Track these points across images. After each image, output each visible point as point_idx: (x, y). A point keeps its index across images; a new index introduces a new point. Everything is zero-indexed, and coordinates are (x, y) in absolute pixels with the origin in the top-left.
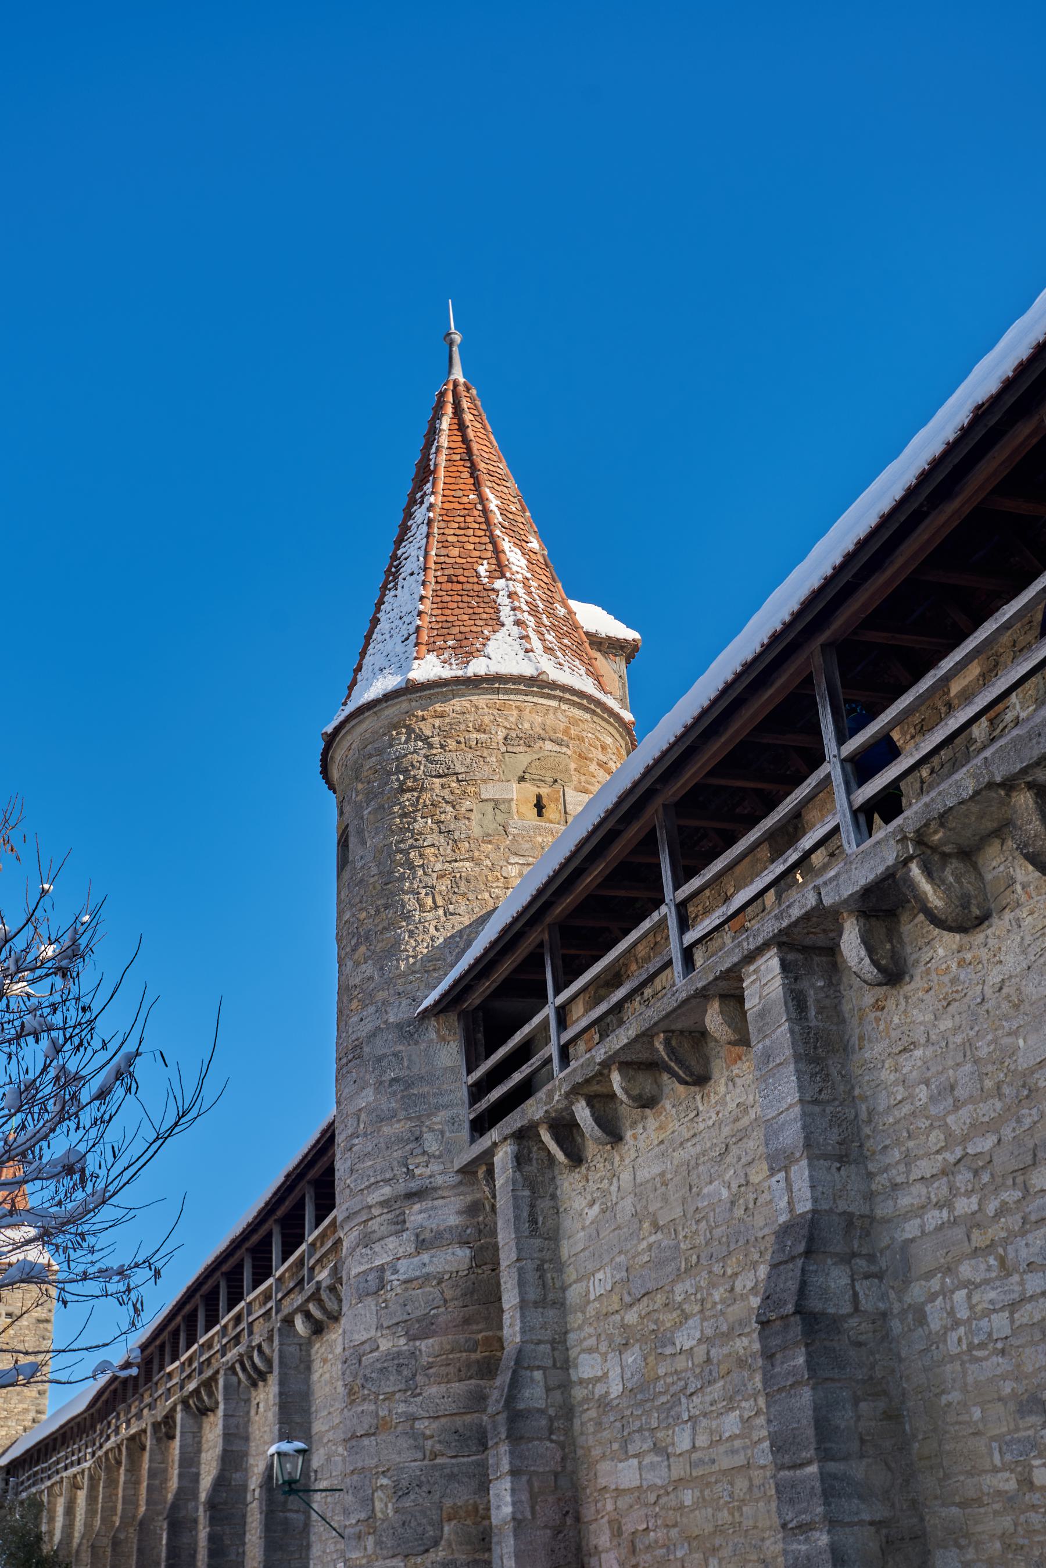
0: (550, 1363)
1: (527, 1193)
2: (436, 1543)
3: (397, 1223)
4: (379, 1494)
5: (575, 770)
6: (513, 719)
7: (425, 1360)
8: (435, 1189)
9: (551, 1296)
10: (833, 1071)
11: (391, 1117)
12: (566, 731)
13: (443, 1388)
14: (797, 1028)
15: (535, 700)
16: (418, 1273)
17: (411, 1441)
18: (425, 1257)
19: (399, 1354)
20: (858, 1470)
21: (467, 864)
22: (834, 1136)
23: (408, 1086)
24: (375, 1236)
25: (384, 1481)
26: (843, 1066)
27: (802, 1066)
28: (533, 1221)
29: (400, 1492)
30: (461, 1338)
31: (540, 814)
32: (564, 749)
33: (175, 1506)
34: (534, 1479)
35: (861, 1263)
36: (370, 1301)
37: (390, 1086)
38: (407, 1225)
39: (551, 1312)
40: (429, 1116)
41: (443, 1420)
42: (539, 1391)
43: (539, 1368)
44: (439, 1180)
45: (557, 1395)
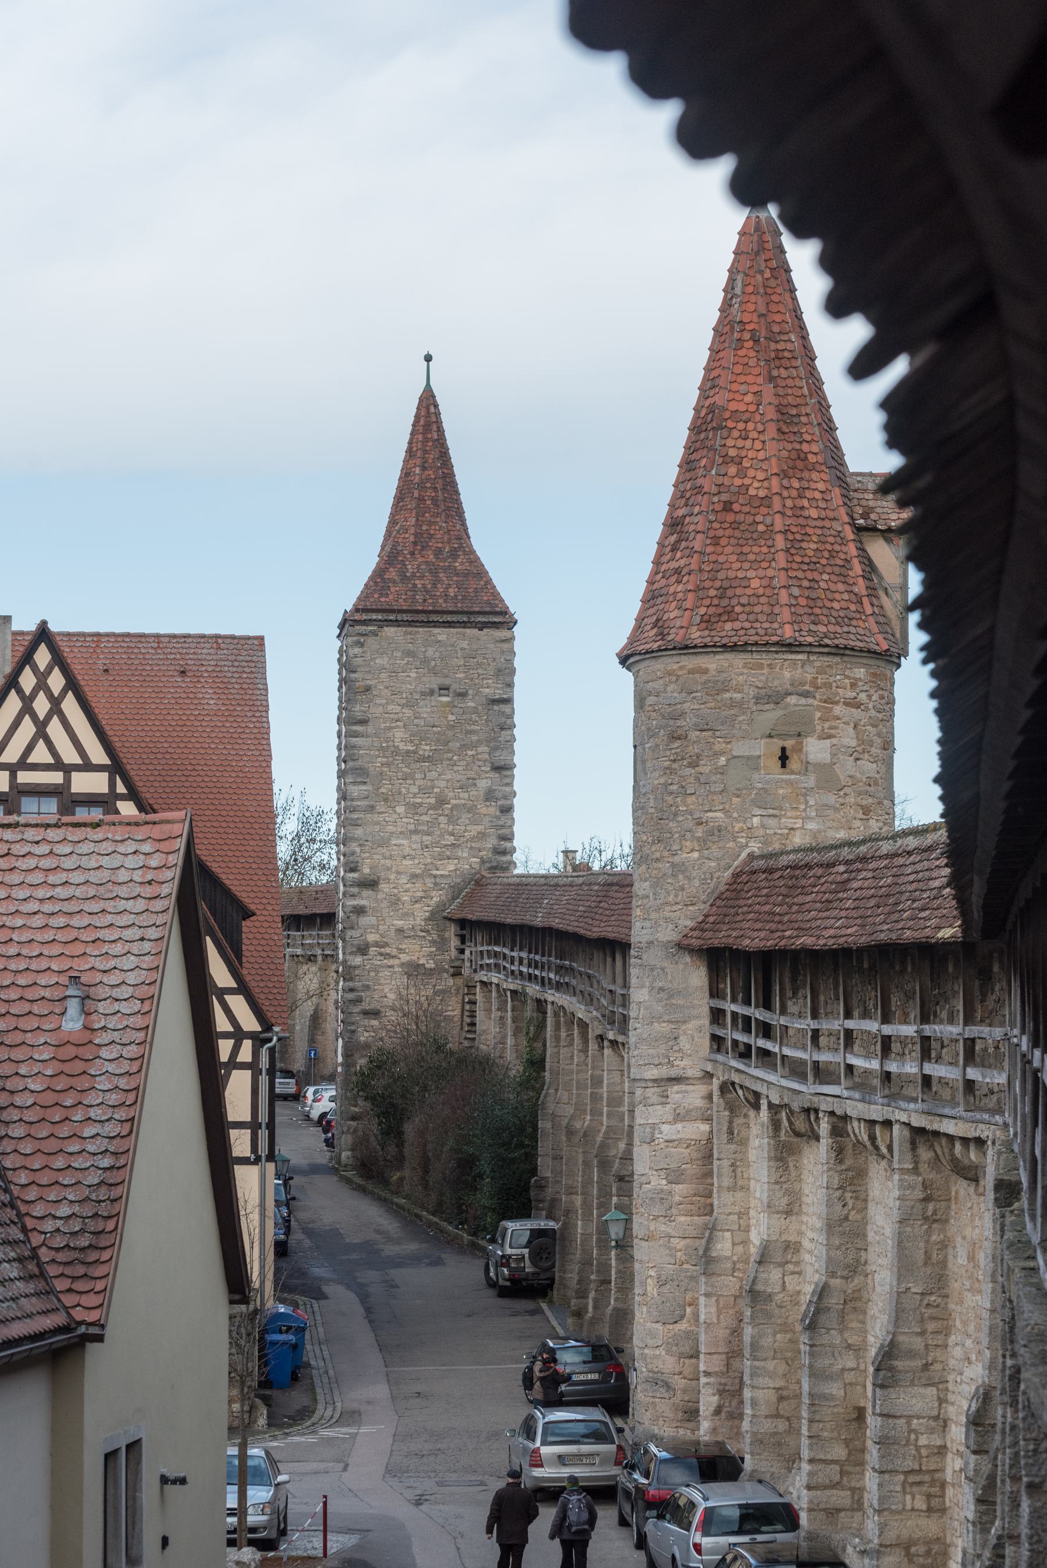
0: (737, 1227)
1: (727, 1113)
2: (682, 1317)
3: (663, 1096)
4: (649, 1280)
5: (819, 719)
6: (763, 678)
7: (677, 1198)
8: (687, 1078)
9: (740, 1183)
10: (791, 1164)
11: (659, 1019)
12: (813, 683)
13: (688, 1218)
14: (772, 1142)
15: (785, 657)
16: (674, 1137)
17: (668, 1251)
18: (679, 1126)
19: (662, 1190)
20: (770, 1365)
21: (719, 814)
22: (785, 1201)
23: (671, 997)
24: (650, 1101)
25: (652, 1273)
26: (797, 1161)
27: (772, 1163)
28: (730, 1132)
29: (661, 1283)
30: (701, 1187)
31: (783, 766)
32: (810, 701)
33: (603, 1146)
34: (721, 1299)
35: (790, 1267)
36: (645, 1146)
37: (659, 993)
38: (669, 1100)
39: (739, 1195)
40: (685, 1022)
41: (688, 1240)
42: (728, 1245)
43: (728, 1230)
44: (690, 1073)
45: (740, 1249)
